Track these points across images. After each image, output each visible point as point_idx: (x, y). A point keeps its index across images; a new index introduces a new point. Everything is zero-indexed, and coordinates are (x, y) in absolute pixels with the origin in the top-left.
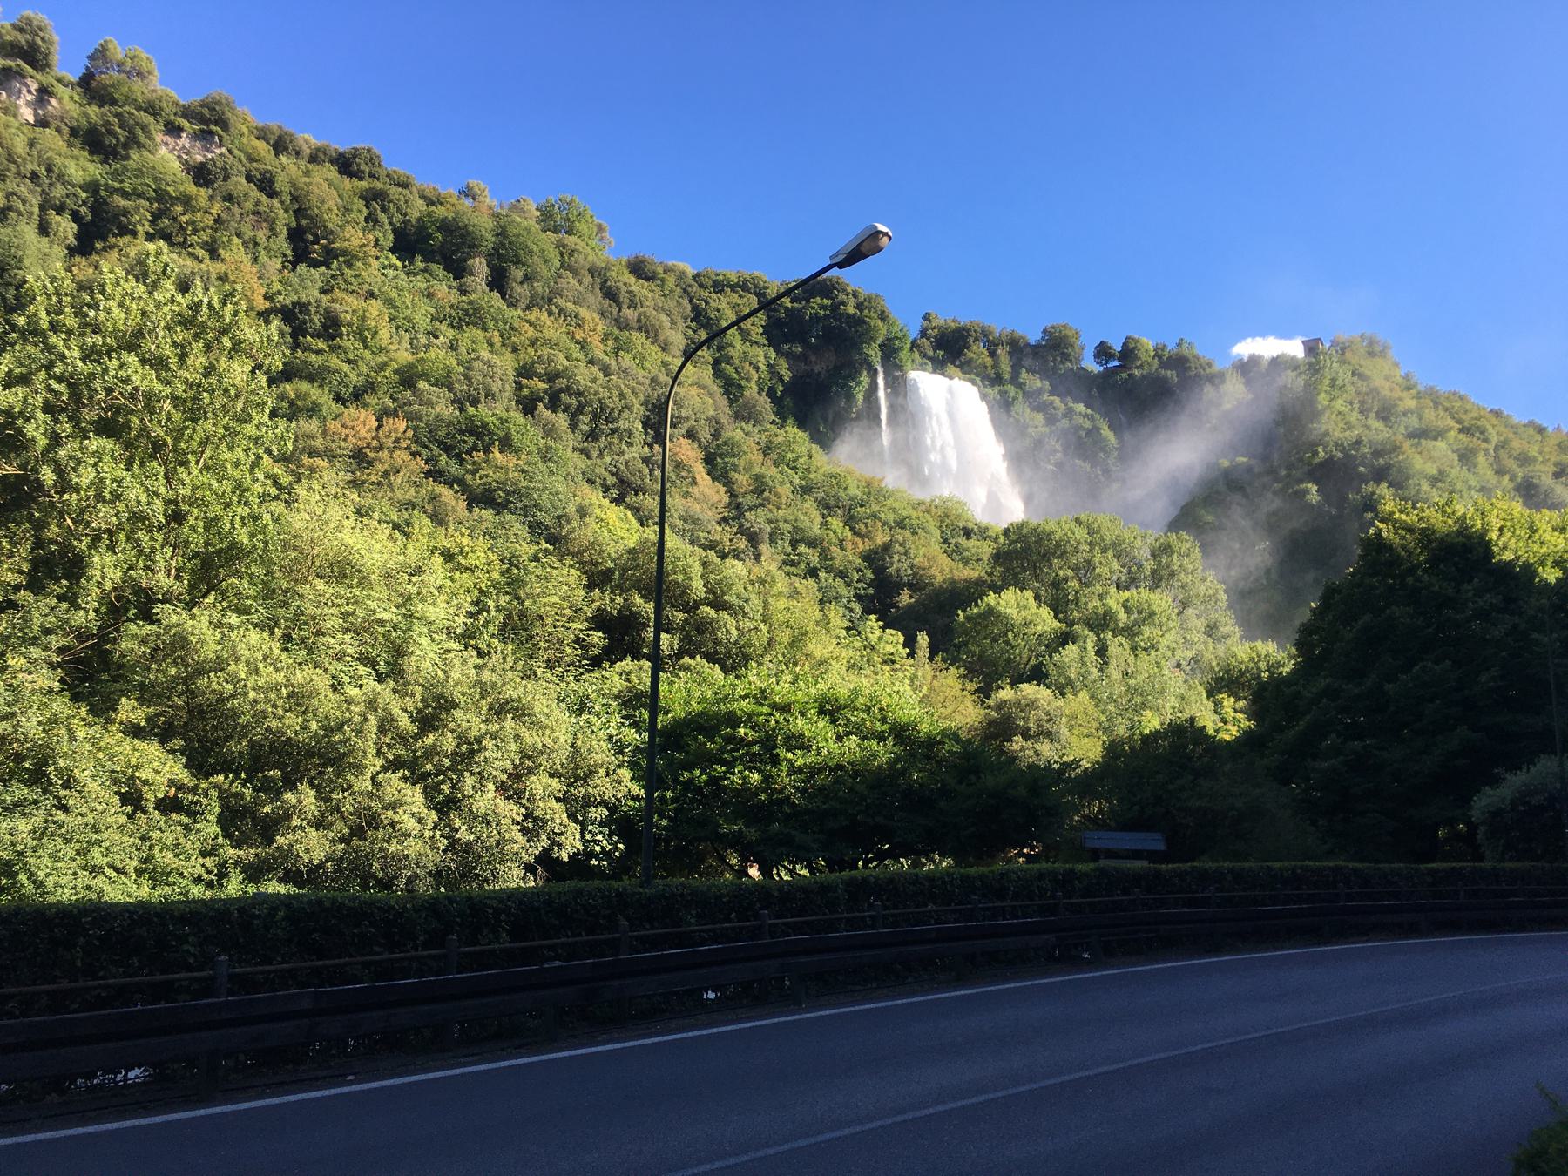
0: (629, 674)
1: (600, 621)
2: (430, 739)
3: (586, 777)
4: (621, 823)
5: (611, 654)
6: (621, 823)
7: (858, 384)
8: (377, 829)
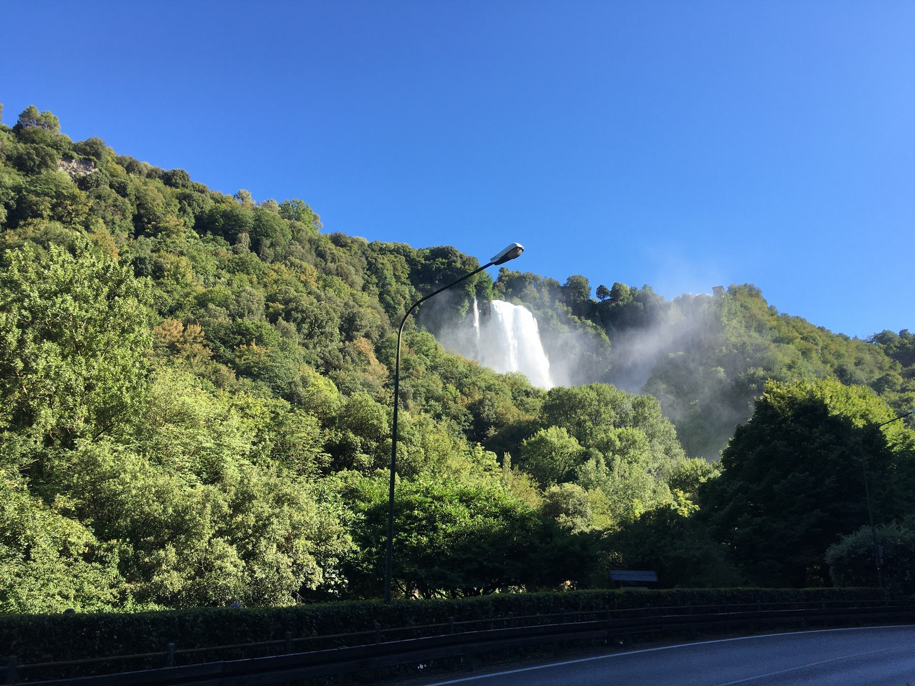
0: (346, 478)
1: (329, 447)
2: (239, 518)
3: (326, 539)
4: (346, 567)
5: (337, 466)
6: (346, 567)
7: (463, 307)
8: (211, 571)
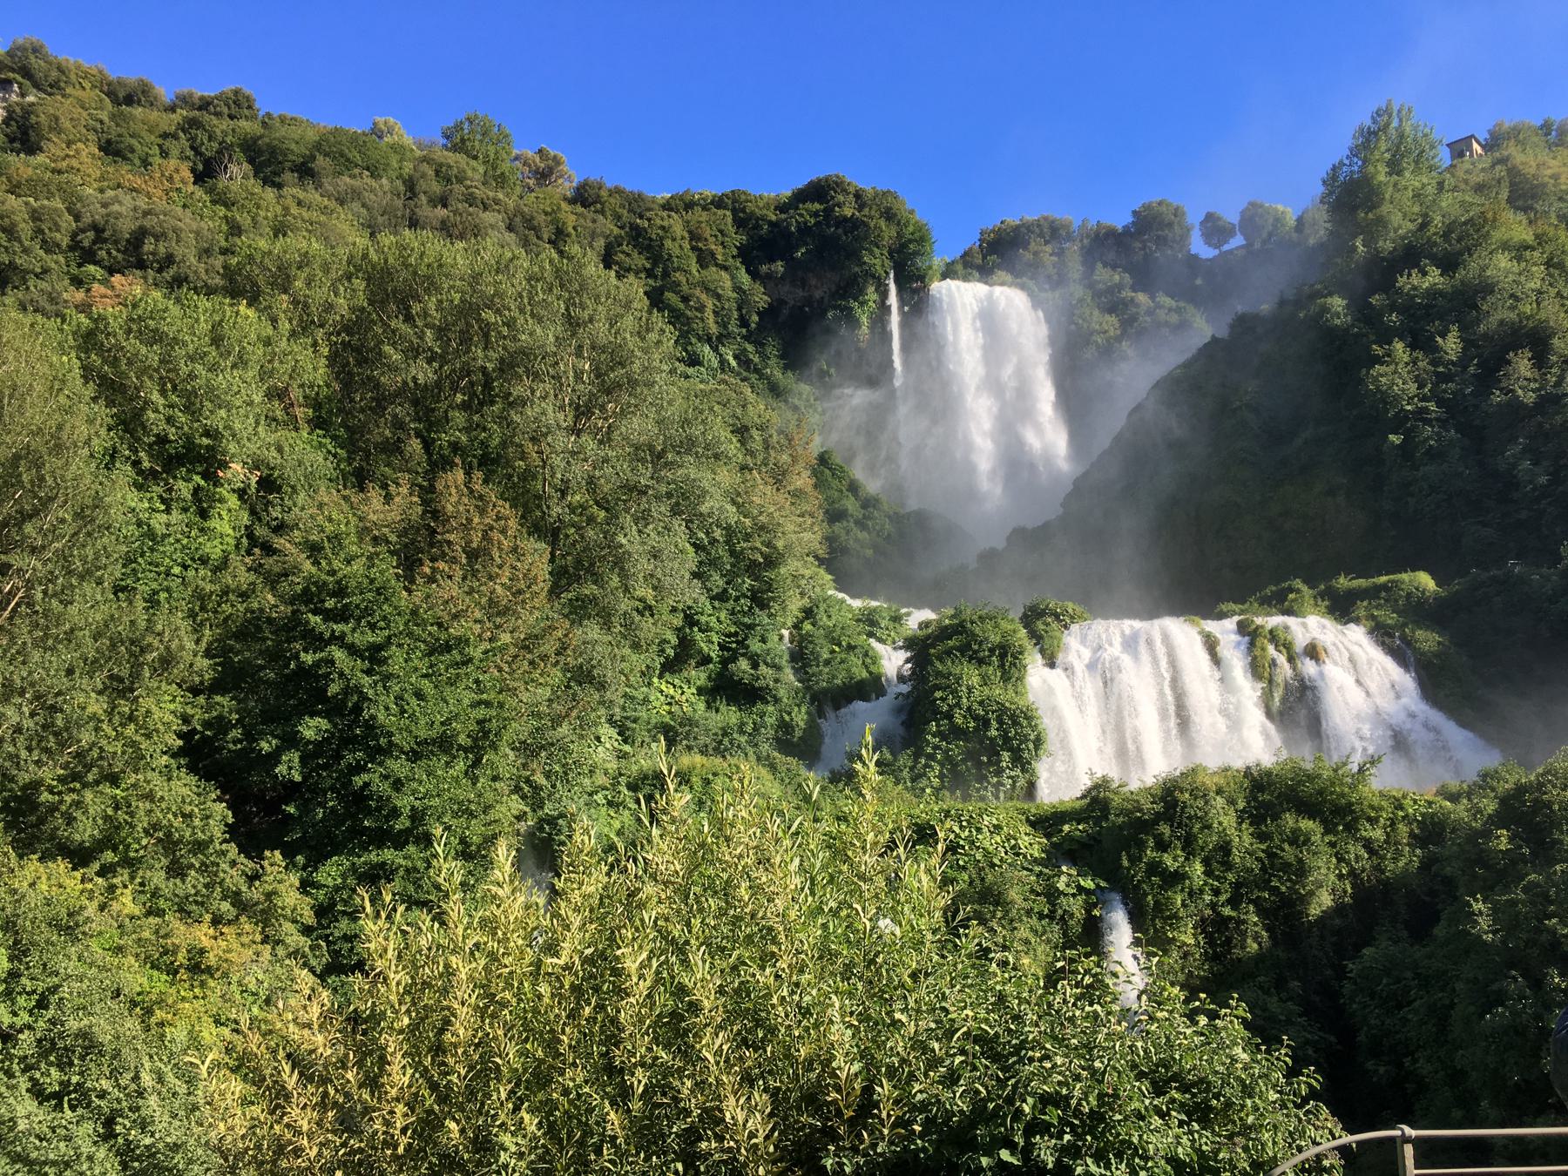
7: (862, 304)
